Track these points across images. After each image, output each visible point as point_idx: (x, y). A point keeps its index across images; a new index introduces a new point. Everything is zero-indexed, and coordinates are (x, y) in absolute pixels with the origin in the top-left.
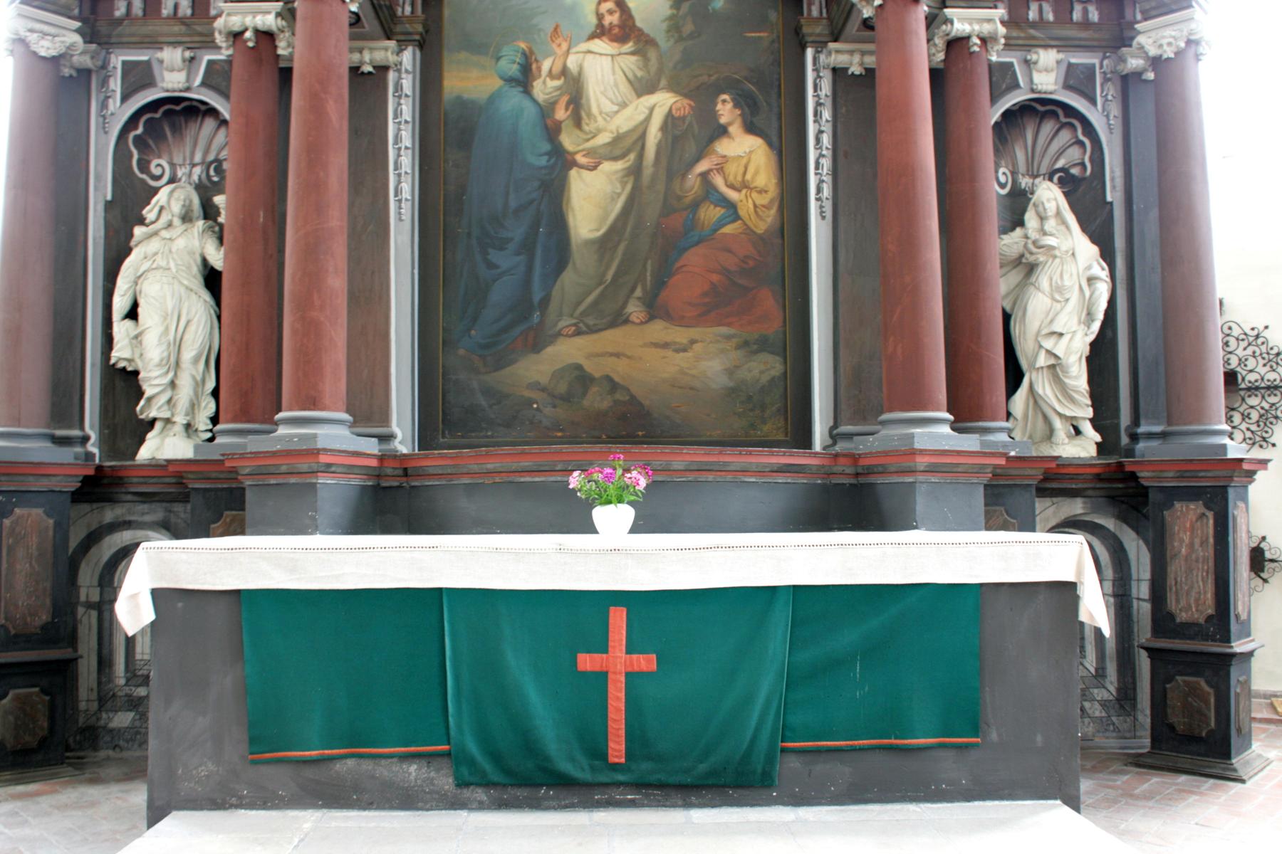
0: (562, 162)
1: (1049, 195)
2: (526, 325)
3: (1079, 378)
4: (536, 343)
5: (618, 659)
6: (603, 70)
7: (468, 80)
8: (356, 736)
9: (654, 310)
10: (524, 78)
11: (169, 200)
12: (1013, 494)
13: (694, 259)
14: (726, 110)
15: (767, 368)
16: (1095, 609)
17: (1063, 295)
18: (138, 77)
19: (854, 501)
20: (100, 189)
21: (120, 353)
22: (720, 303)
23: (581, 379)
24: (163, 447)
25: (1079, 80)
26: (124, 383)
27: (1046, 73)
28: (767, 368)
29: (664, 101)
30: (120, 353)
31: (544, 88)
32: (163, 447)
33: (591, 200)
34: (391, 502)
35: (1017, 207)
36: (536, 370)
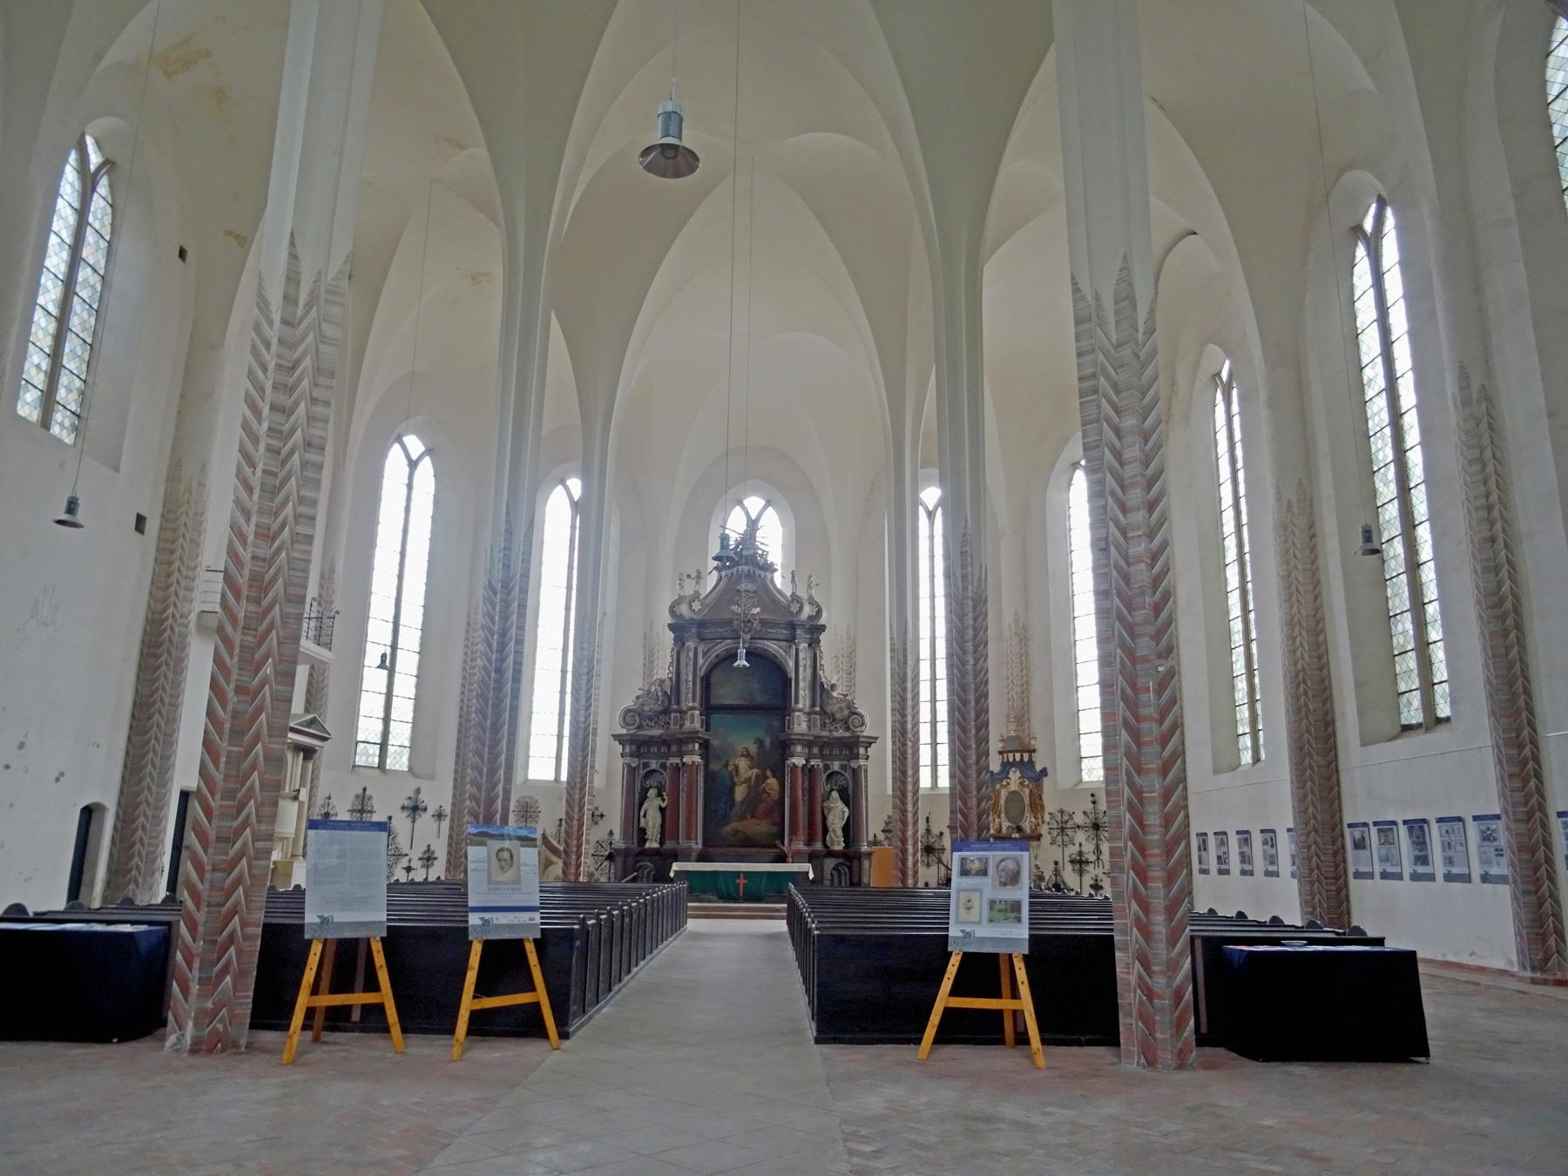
0: (734, 784)
1: (835, 794)
2: (725, 819)
3: (840, 833)
4: (728, 823)
5: (742, 881)
6: (743, 764)
7: (714, 766)
8: (704, 891)
9: (753, 816)
10: (726, 765)
11: (652, 793)
12: (812, 858)
13: (762, 806)
14: (769, 773)
15: (775, 829)
16: (811, 876)
17: (838, 813)
18: (646, 765)
19: (782, 859)
20: (638, 789)
21: (642, 824)
22: (768, 814)
23: (738, 831)
24: (652, 844)
25: (843, 767)
26: (643, 831)
27: (836, 766)
28: (775, 829)
29: (756, 771)
30: (642, 824)
31: (730, 768)
32: (652, 844)
33: (740, 793)
34: (702, 858)
35: (827, 797)
36: (729, 828)
